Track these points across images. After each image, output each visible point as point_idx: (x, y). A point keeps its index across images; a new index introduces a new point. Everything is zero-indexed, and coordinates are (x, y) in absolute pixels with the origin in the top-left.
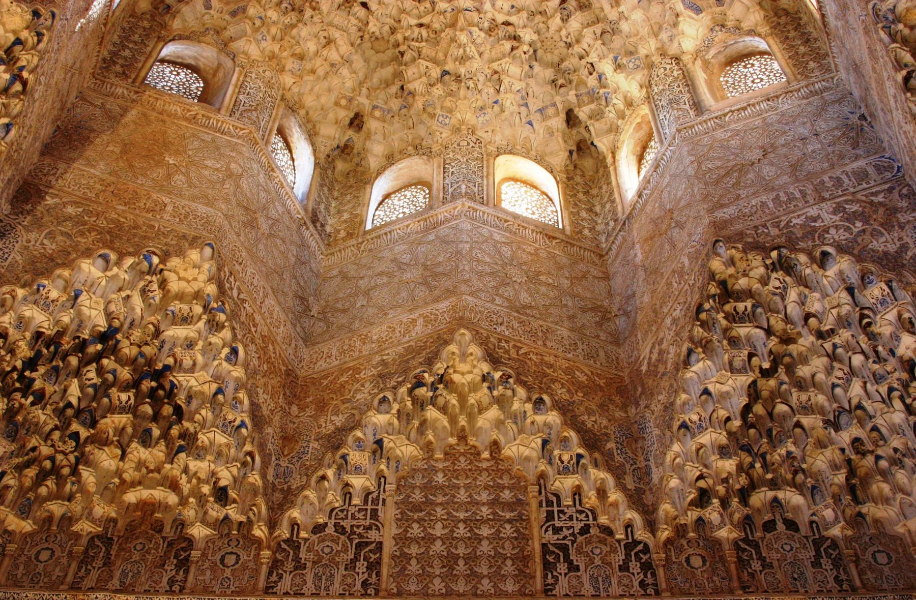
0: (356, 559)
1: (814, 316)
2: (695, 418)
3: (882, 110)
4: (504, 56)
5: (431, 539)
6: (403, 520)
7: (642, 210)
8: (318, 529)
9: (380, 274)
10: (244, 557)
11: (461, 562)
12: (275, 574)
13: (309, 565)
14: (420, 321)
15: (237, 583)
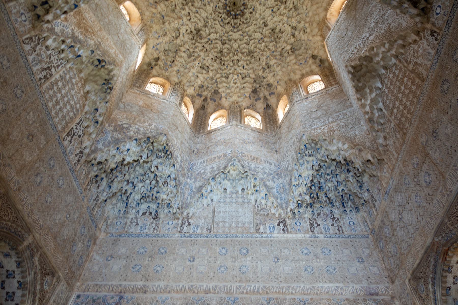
0: (45, 69)
1: (157, 168)
2: (121, 150)
3: (204, 161)
4: (171, 34)
5: (60, 91)
6: (61, 77)
7: (150, 98)
8: (47, 48)
9: (115, 24)
10: (27, 23)
11: (59, 107)
12: (28, 41)
13: (36, 53)
14: (113, 51)
15: (18, 27)
